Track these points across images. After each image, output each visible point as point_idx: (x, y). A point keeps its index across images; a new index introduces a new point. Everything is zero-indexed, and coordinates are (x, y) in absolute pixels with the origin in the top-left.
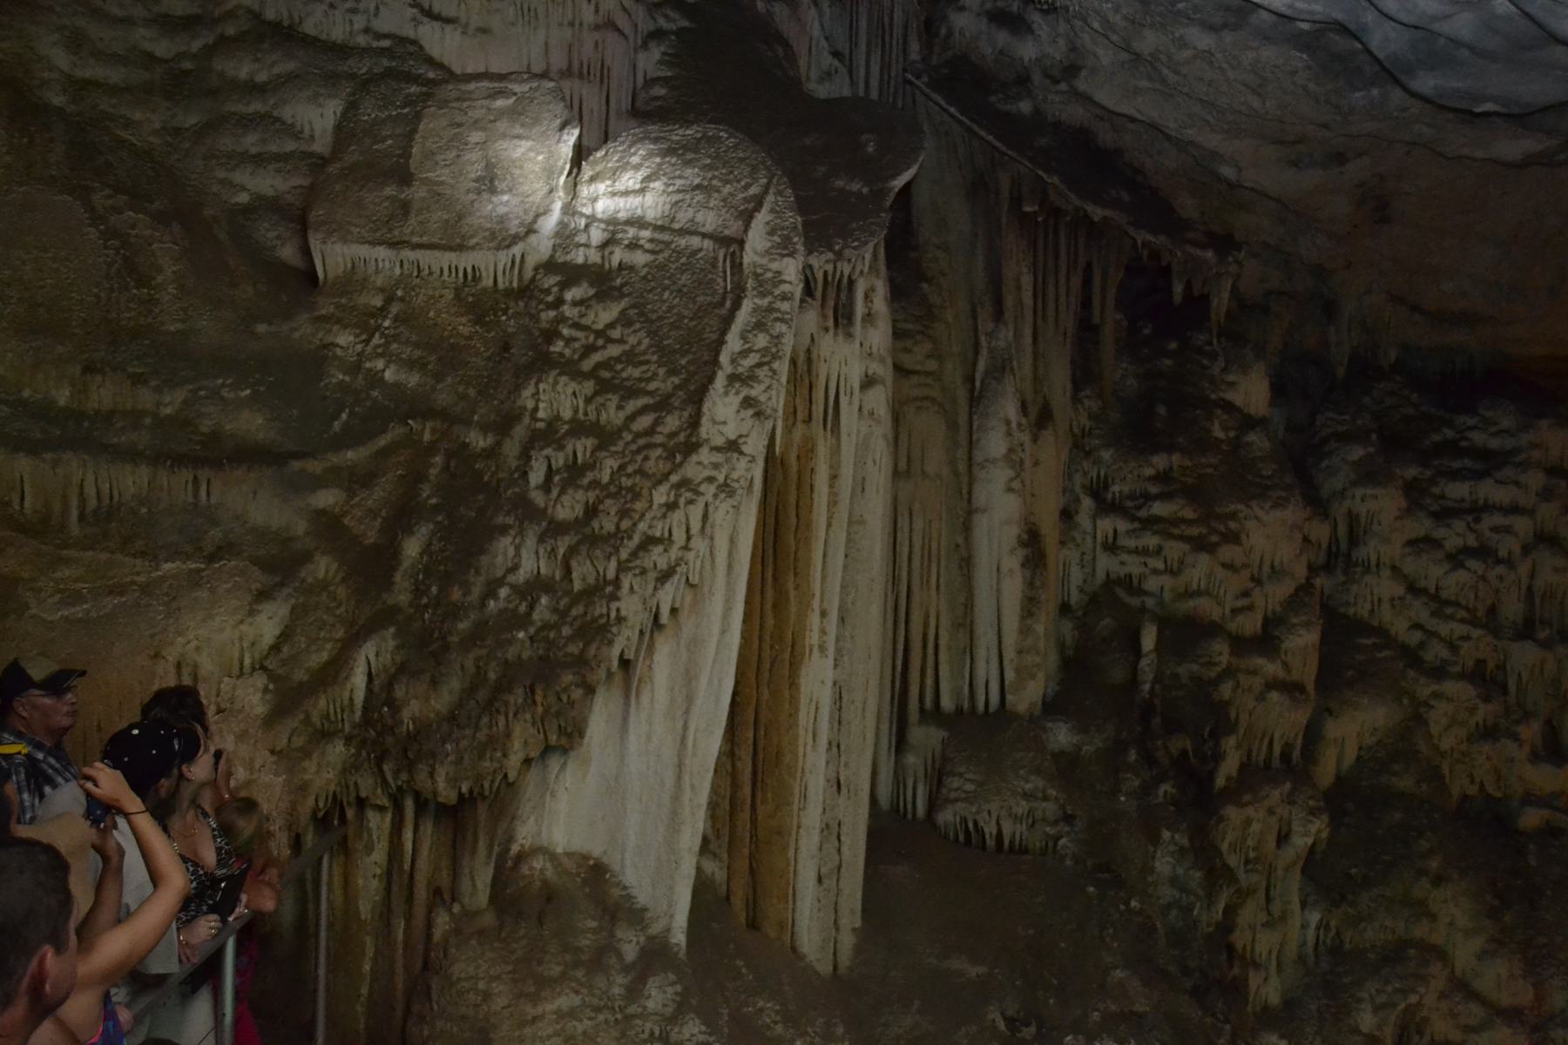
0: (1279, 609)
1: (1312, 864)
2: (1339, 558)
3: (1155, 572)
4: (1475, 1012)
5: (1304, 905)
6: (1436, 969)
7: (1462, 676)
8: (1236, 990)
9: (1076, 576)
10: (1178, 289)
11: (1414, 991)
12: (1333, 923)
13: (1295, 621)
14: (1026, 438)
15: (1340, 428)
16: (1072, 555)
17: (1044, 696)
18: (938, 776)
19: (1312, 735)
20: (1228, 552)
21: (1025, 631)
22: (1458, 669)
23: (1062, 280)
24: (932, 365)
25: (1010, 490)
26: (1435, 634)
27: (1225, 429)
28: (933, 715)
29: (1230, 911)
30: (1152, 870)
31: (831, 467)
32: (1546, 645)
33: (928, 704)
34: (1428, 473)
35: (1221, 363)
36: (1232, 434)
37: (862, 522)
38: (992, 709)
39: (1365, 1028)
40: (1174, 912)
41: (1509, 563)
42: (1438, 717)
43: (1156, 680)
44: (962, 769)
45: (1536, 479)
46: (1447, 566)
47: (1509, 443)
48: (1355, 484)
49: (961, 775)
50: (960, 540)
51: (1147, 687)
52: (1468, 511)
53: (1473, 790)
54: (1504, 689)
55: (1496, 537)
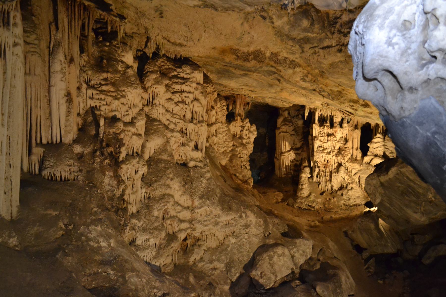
0: (135, 115)
1: (143, 178)
2: (150, 103)
3: (103, 105)
4: (179, 208)
5: (141, 188)
6: (171, 200)
7: (178, 131)
8: (125, 210)
9: (82, 105)
10: (109, 28)
11: (166, 205)
12: (148, 192)
13: (139, 118)
14: (67, 66)
15: (150, 70)
16: (80, 100)
17: (73, 138)
18: (42, 162)
19: (143, 146)
20: (122, 100)
21: (67, 120)
22: (177, 130)
23: (77, 22)
24: (36, 42)
25: (62, 80)
27: (122, 68)
28: (40, 144)
29: (124, 191)
30: (104, 182)
31: (3, 70)
32: (196, 124)
33: (38, 141)
34: (171, 82)
35: (120, 50)
36: (123, 69)
37: (15, 87)
38: (58, 143)
39: (155, 215)
40: (109, 192)
41: (188, 105)
42: (172, 142)
43: (104, 133)
44: (50, 159)
45: (194, 85)
46: (175, 105)
47: (188, 76)
48: (154, 84)
49: (49, 161)
50: (47, 95)
51: (102, 135)
52: (179, 92)
53: (180, 158)
54: (187, 134)
55: (185, 99)
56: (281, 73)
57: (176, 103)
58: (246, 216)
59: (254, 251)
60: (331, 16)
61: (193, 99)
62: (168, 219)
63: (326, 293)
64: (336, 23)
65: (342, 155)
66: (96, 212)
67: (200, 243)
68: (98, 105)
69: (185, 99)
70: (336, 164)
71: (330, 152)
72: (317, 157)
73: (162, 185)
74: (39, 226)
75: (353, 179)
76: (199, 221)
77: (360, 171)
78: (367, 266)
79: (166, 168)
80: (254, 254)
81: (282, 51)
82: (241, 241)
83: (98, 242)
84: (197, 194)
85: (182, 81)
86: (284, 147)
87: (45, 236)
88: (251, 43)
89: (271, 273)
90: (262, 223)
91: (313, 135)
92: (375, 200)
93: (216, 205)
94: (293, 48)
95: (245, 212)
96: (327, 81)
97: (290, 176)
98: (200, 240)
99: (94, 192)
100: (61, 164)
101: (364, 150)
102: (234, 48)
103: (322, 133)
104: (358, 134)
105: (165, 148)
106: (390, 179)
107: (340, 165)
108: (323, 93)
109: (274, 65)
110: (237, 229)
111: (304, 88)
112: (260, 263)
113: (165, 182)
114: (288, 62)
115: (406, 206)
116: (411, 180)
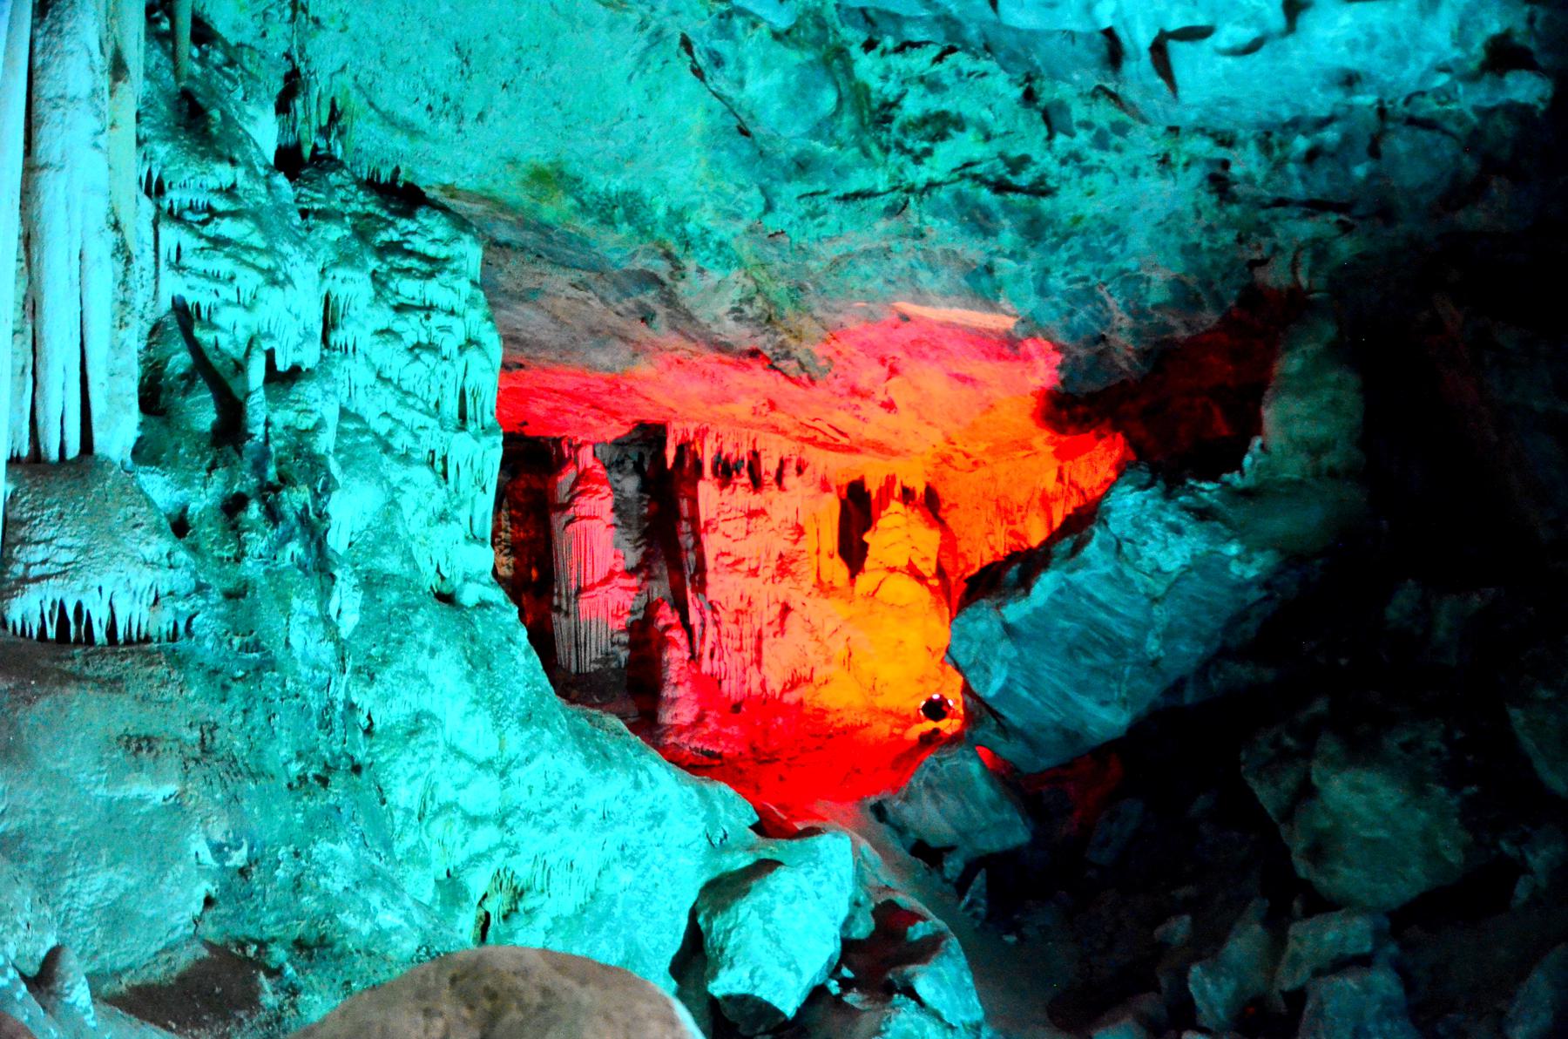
3: (228, 303)
7: (420, 463)
15: (316, 206)
21: (118, 347)
25: (96, 146)
26: (400, 422)
43: (268, 424)
44: (49, 534)
45: (464, 286)
46: (408, 358)
47: (443, 253)
48: (335, 265)
54: (445, 475)
55: (442, 335)
56: (682, 287)
57: (411, 350)
58: (651, 779)
59: (689, 905)
60: (873, 96)
61: (463, 342)
62: (436, 815)
63: (944, 996)
64: (889, 119)
65: (793, 574)
66: (303, 779)
67: (526, 904)
68: (205, 301)
69: (438, 337)
70: (777, 609)
71: (757, 569)
72: (719, 586)
73: (405, 674)
74: (113, 863)
75: (828, 649)
76: (528, 816)
77: (849, 619)
78: (967, 898)
79: (406, 606)
80: (693, 914)
81: (702, 204)
82: (648, 875)
83: (367, 913)
84: (512, 707)
85: (425, 267)
86: (589, 567)
87: (149, 913)
88: (632, 158)
89: (781, 965)
90: (696, 800)
91: (694, 518)
92: (987, 683)
93: (569, 744)
94: (741, 195)
95: (643, 768)
96: (806, 322)
97: (614, 665)
98: (529, 889)
99: (272, 689)
100: (113, 556)
101: (853, 553)
102: (569, 170)
103: (726, 508)
104: (830, 507)
105: (387, 528)
106: (1036, 610)
107: (786, 609)
108: (782, 364)
109: (677, 250)
110: (628, 833)
111: (721, 348)
112: (731, 943)
113: (414, 664)
114: (711, 245)
115: (1082, 688)
116: (1101, 605)
